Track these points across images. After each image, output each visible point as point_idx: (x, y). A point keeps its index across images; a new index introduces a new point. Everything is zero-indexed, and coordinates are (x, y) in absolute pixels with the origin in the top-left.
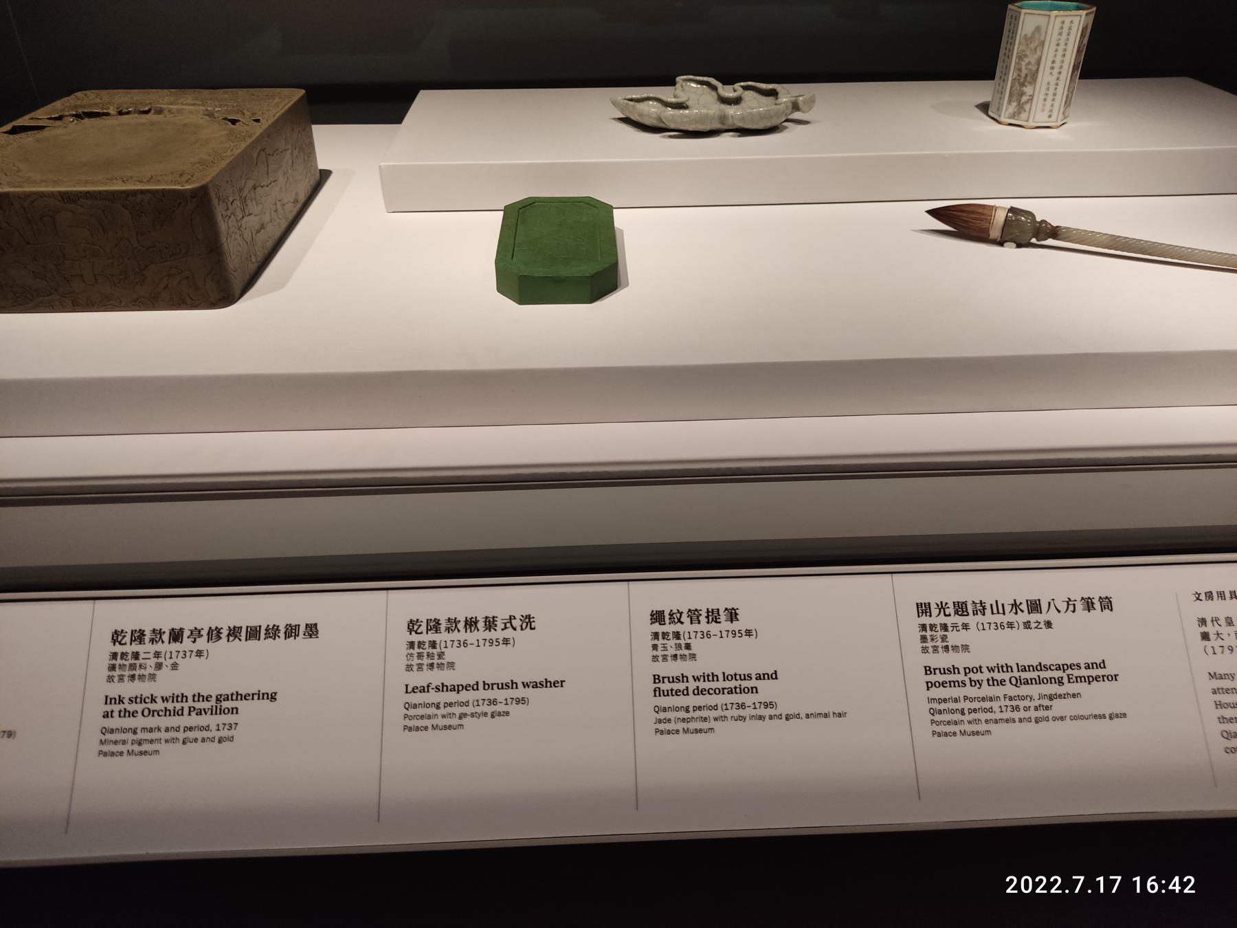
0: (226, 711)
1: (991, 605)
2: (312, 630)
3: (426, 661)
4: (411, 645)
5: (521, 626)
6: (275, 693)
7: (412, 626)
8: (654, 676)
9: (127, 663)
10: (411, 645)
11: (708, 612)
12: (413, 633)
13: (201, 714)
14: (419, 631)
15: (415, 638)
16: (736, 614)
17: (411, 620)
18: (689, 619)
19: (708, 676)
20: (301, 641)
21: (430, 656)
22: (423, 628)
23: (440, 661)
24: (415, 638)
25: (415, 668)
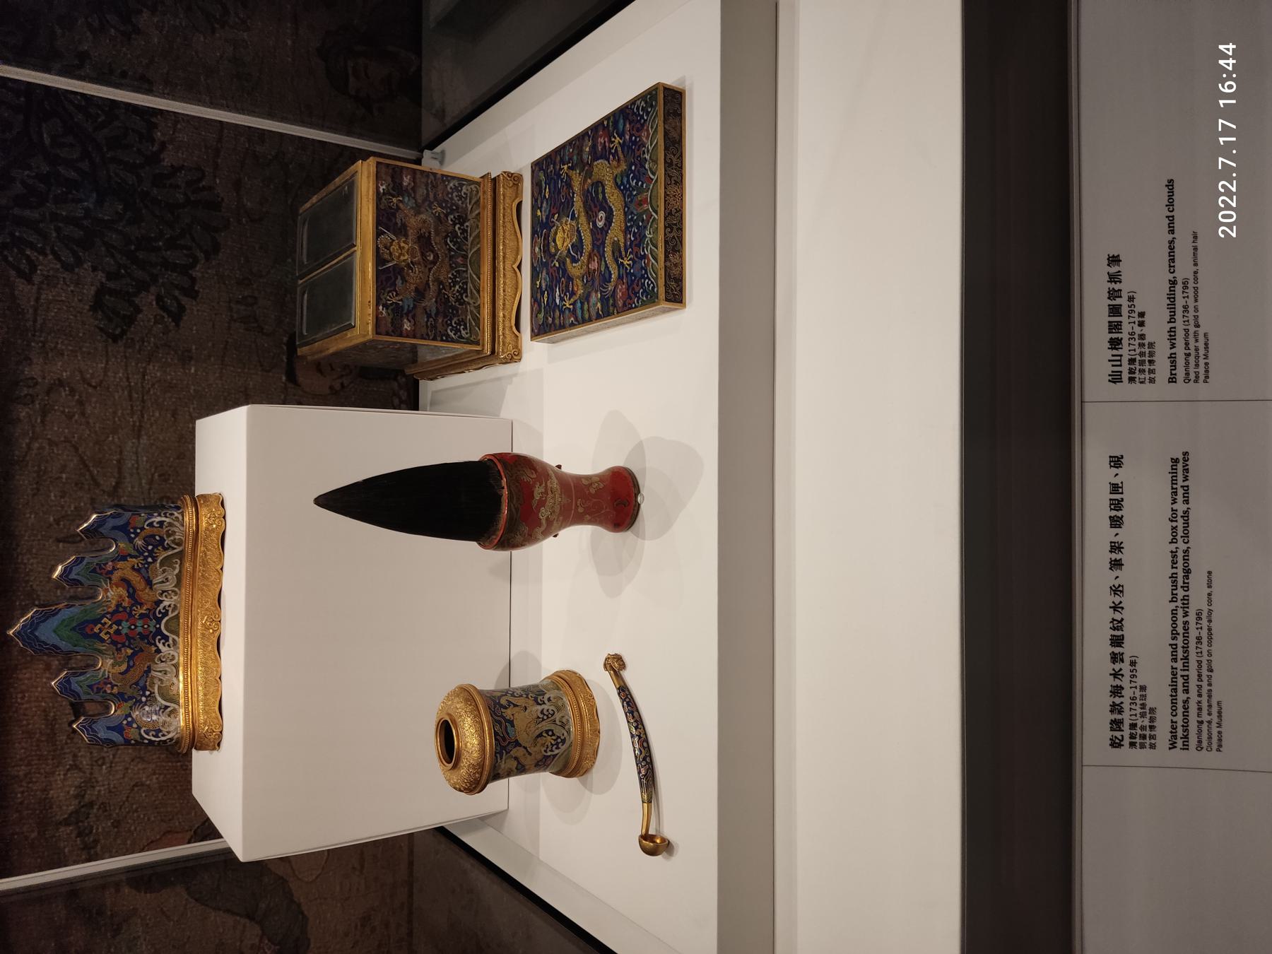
0: (1186, 532)
1: (1113, 366)
2: (1114, 260)
3: (1147, 367)
4: (1132, 745)
5: (1120, 697)
6: (1172, 459)
7: (1116, 744)
8: (1169, 382)
9: (1138, 367)
10: (1132, 745)
11: (1111, 282)
12: (1122, 743)
13: (1188, 469)
14: (1120, 738)
15: (1127, 741)
16: (1113, 256)
17: (1110, 711)
18: (1117, 299)
19: (1170, 336)
20: (1126, 600)
21: (1142, 363)
22: (1118, 734)
23: (1147, 355)
24: (1127, 741)
25: (1152, 376)
